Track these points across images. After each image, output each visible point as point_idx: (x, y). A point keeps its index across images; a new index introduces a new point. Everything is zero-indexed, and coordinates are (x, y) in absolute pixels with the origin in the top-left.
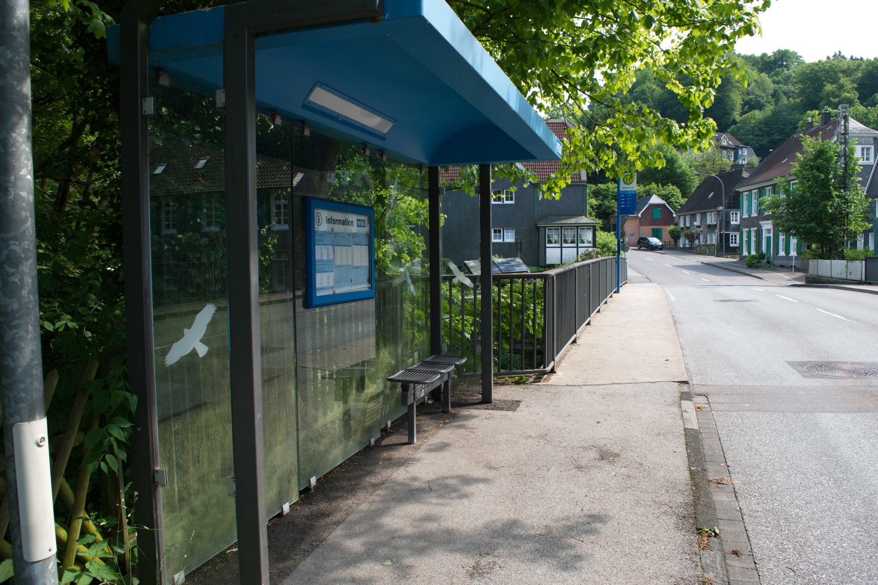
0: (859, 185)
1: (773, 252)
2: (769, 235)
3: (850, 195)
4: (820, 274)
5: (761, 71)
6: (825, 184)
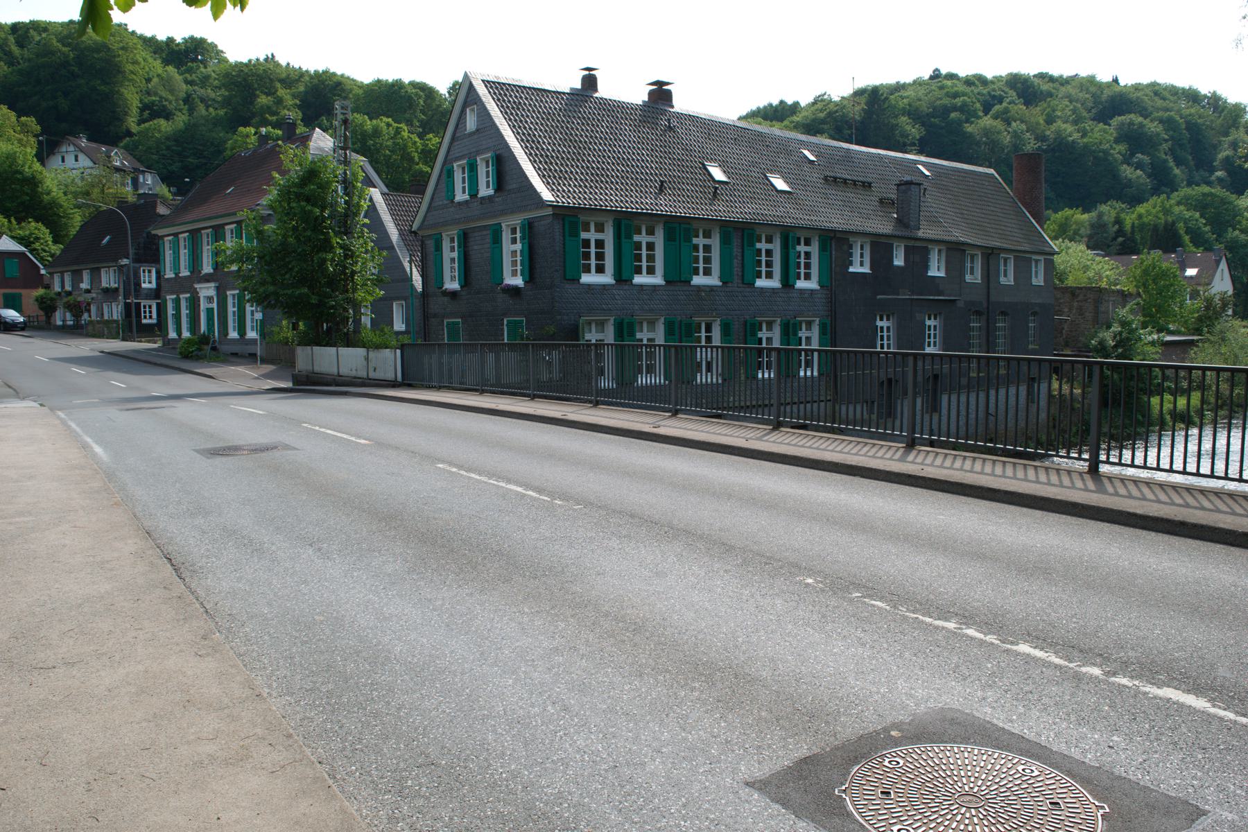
0: (366, 230)
1: (219, 332)
2: (210, 306)
3: (356, 245)
4: (317, 369)
5: (166, 62)
6: (316, 225)
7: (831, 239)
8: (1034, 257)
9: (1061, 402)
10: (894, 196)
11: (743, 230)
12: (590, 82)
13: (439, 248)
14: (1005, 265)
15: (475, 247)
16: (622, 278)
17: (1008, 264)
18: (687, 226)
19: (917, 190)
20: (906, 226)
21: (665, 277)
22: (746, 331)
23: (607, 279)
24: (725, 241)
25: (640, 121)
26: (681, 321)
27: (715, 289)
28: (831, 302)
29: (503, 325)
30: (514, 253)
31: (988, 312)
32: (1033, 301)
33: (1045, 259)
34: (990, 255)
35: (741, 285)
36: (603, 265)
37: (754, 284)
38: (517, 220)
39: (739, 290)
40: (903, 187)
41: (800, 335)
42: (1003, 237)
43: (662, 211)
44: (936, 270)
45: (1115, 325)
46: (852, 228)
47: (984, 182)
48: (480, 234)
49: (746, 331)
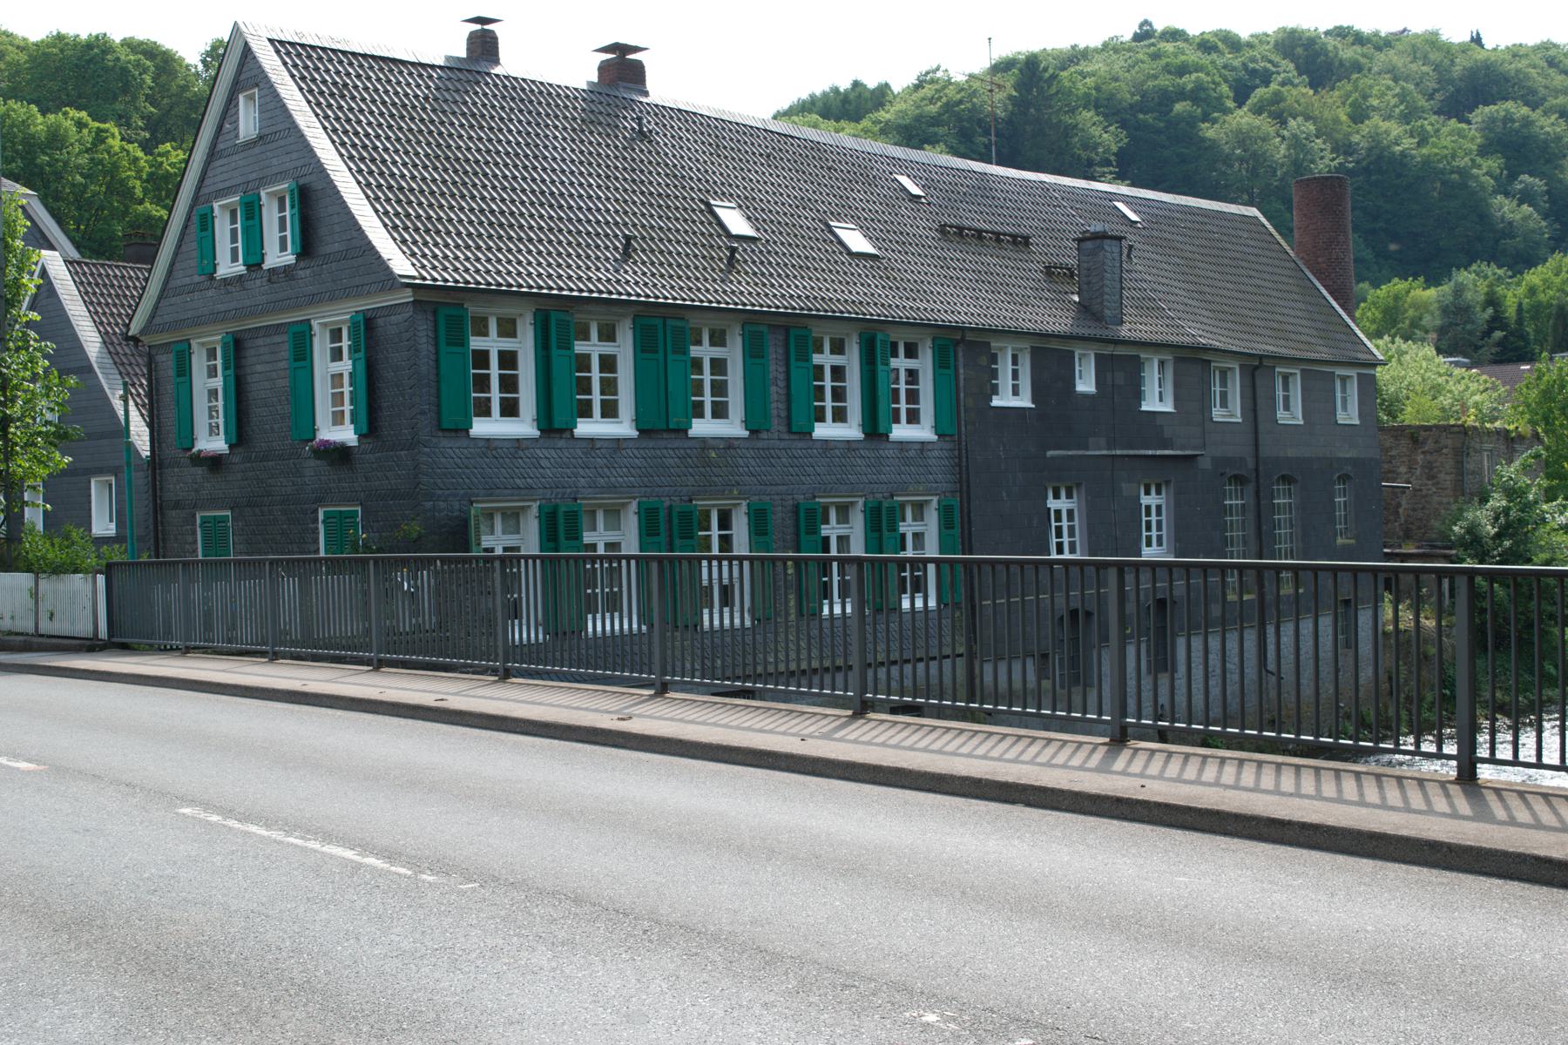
0: (32, 334)
7: (957, 343)
8: (1340, 371)
9: (1400, 643)
10: (1073, 262)
11: (787, 329)
12: (484, 44)
13: (184, 369)
14: (1286, 388)
15: (258, 368)
16: (552, 426)
17: (1291, 385)
18: (679, 323)
19: (1116, 250)
20: (1098, 318)
21: (638, 421)
22: (797, 526)
23: (523, 427)
24: (753, 352)
25: (583, 121)
26: (670, 508)
27: (736, 443)
28: (960, 466)
29: (316, 520)
30: (337, 379)
32: (1341, 455)
33: (1358, 374)
34: (1257, 368)
35: (786, 436)
36: (516, 401)
37: (810, 434)
38: (342, 313)
39: (782, 445)
40: (1089, 245)
41: (902, 530)
43: (629, 294)
44: (1157, 400)
46: (996, 323)
47: (1241, 233)
48: (268, 340)
49: (797, 526)
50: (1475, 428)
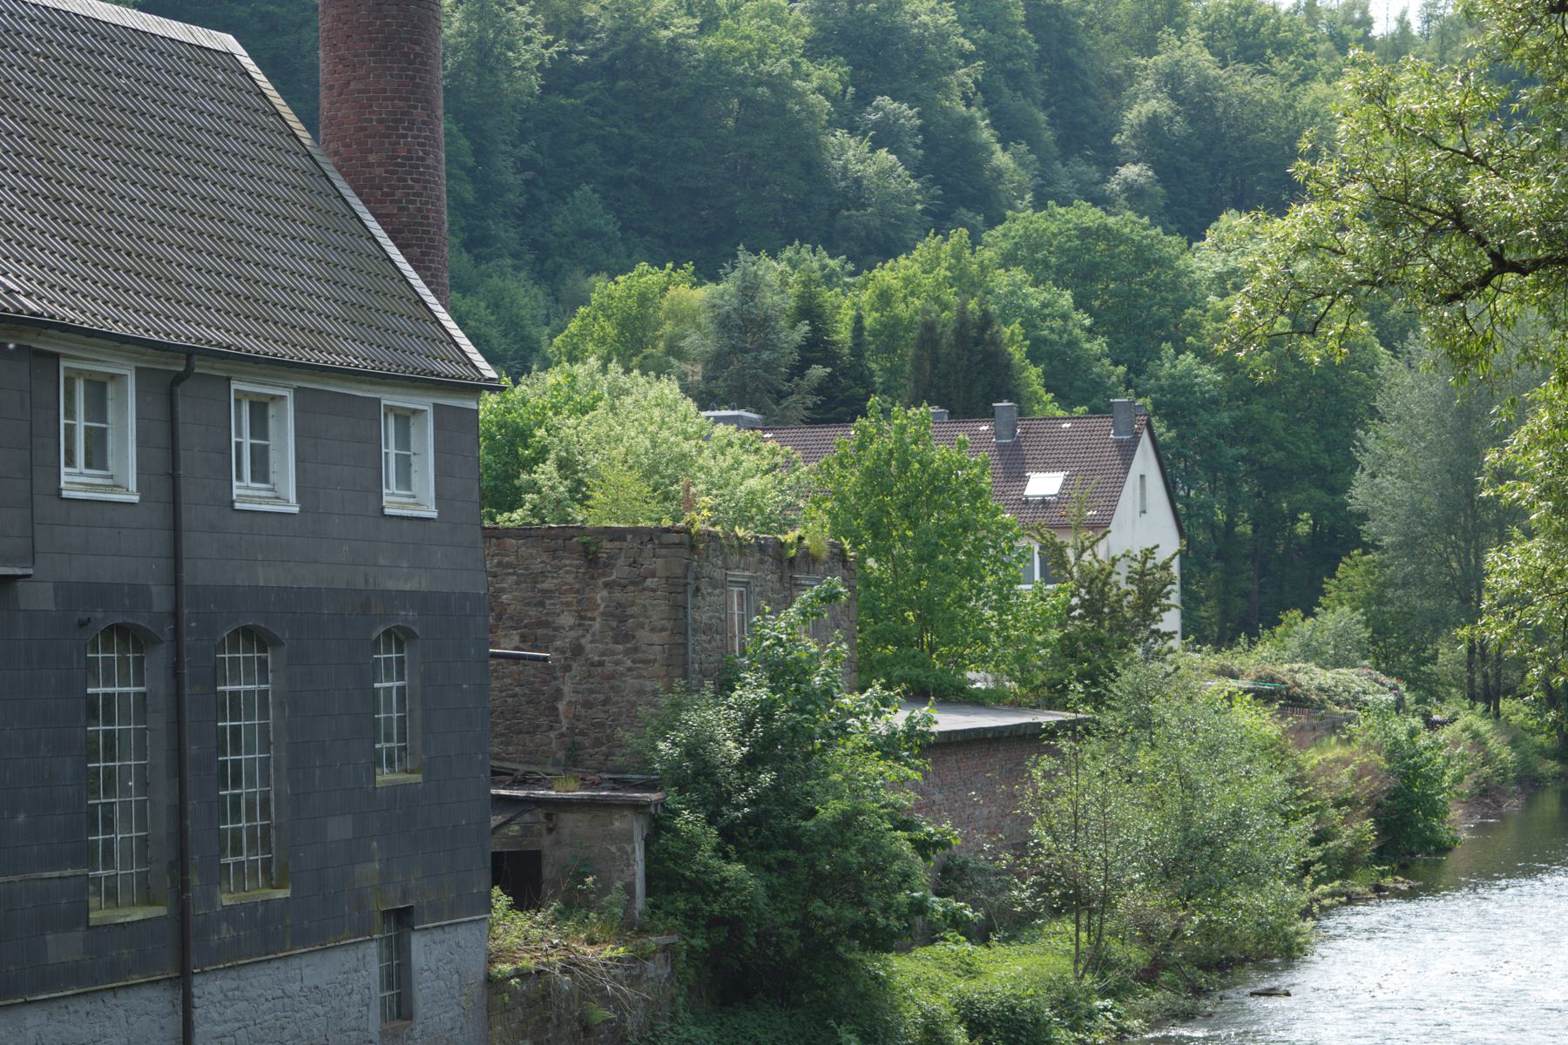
8: (391, 398)
17: (272, 424)
31: (177, 631)
32: (391, 585)
33: (435, 406)
42: (250, 307)
45: (749, 677)
47: (186, 83)
50: (713, 537)
